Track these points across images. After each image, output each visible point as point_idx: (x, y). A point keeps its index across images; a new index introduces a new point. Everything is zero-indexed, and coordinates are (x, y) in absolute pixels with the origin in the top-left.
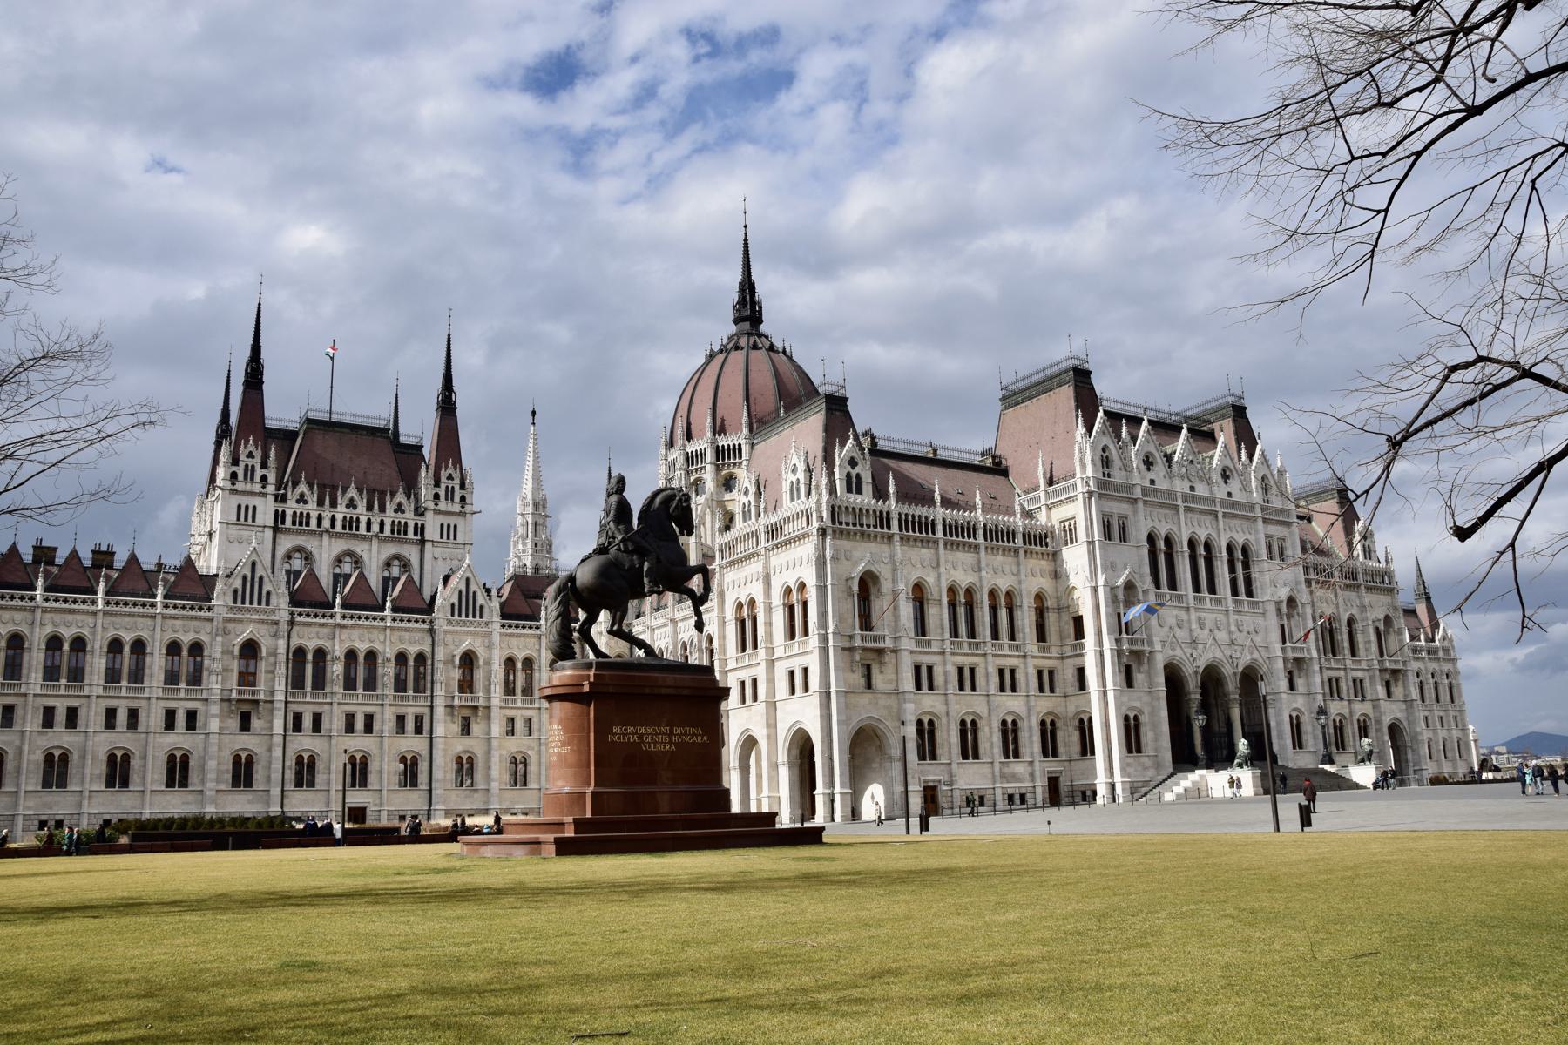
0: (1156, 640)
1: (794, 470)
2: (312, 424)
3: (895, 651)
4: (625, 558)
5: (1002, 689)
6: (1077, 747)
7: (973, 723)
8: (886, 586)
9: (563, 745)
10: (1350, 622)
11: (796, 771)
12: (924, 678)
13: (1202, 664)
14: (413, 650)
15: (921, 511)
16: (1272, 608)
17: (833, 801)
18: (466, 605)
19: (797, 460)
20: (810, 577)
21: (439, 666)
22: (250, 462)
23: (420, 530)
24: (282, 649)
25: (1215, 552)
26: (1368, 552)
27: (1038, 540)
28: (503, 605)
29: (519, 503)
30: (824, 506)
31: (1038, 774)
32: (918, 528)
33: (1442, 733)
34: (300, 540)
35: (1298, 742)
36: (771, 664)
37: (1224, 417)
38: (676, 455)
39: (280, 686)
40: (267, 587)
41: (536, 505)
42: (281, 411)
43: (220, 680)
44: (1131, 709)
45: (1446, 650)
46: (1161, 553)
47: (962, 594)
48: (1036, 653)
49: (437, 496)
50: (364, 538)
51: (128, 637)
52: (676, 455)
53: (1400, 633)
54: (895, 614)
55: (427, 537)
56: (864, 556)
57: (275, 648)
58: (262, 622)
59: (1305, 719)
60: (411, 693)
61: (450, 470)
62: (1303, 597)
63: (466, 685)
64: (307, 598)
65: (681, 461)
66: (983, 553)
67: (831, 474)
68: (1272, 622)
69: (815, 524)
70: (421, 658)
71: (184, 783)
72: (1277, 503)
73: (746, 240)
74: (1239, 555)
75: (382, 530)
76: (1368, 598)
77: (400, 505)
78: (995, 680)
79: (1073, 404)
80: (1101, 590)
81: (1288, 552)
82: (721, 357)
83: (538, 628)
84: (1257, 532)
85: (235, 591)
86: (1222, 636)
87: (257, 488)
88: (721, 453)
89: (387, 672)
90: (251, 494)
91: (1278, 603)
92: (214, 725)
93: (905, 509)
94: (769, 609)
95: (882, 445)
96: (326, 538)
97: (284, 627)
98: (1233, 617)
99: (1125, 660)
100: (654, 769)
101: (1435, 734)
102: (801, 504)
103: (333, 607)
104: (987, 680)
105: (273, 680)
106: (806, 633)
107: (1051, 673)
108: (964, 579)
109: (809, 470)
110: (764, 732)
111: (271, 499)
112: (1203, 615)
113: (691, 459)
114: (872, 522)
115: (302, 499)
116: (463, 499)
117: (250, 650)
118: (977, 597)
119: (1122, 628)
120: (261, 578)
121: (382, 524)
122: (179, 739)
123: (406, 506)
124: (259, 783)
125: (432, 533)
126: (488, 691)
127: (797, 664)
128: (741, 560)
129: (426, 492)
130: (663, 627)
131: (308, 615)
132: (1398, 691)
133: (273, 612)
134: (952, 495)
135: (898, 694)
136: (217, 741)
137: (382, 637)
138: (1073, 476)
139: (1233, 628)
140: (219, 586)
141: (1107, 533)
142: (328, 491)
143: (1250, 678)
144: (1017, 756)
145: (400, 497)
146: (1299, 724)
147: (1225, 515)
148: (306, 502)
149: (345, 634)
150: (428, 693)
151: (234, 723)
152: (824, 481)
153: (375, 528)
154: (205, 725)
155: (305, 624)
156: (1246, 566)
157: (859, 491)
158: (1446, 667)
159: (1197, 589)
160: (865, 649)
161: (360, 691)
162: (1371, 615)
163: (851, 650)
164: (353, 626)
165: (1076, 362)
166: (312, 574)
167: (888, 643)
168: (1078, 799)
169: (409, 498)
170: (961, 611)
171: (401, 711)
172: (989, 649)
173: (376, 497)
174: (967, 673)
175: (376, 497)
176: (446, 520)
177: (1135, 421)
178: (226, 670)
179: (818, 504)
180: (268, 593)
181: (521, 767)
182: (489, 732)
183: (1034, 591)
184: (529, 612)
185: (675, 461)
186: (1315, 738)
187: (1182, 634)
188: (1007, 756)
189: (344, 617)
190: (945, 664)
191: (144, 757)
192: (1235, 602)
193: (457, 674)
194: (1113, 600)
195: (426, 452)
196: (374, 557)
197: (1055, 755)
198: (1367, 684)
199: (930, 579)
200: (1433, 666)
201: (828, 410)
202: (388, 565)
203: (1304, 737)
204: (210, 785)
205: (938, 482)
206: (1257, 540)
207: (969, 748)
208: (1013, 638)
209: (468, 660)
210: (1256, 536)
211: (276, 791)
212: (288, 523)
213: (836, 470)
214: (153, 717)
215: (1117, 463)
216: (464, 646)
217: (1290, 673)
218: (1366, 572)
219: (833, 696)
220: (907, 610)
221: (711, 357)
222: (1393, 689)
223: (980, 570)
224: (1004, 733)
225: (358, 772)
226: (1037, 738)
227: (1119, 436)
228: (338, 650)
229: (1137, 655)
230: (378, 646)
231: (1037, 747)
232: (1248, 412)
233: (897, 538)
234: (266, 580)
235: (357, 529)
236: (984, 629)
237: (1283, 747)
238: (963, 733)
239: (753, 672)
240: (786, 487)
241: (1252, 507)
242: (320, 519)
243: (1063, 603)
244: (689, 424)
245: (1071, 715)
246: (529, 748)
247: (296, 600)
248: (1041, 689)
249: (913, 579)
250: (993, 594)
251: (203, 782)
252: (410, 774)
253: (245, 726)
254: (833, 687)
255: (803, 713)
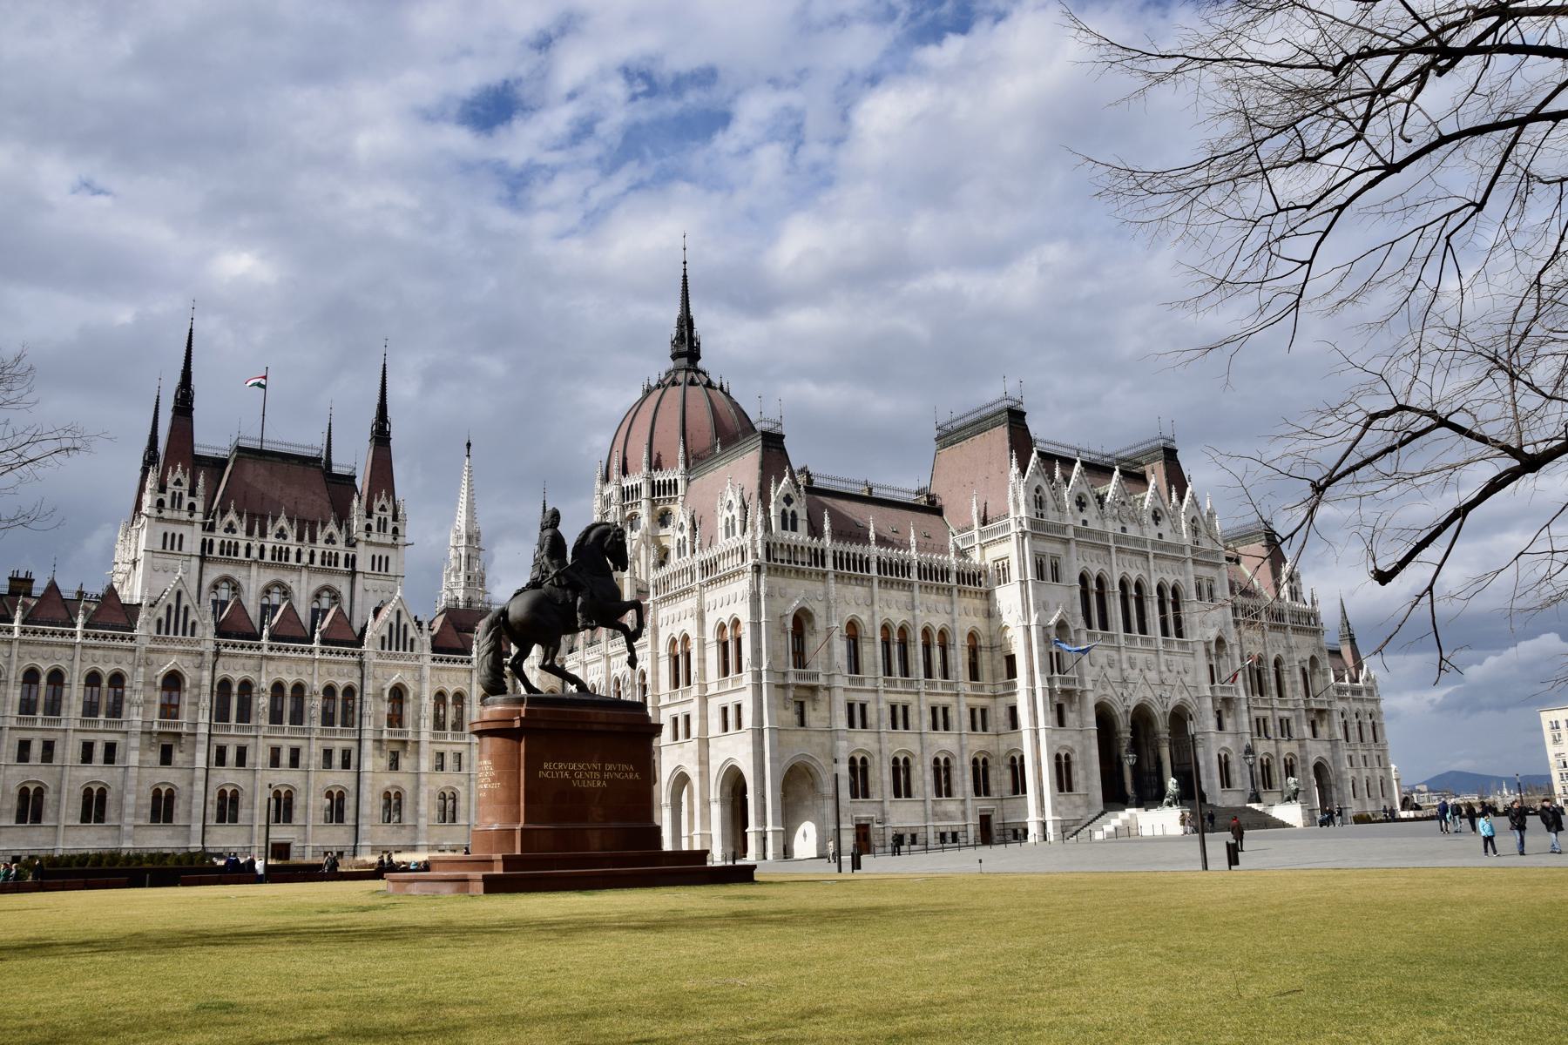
0: (1088, 679)
1: (730, 507)
2: (243, 452)
3: (828, 689)
4: (559, 593)
5: (935, 727)
6: (1008, 786)
7: (906, 761)
8: (820, 623)
9: (493, 780)
10: (1277, 663)
11: (729, 808)
12: (857, 715)
13: (1132, 704)
14: (341, 683)
15: (855, 549)
16: (1201, 649)
17: (765, 839)
18: (397, 638)
19: (733, 497)
20: (744, 613)
21: (368, 699)
22: (177, 489)
23: (351, 561)
24: (207, 681)
25: (1146, 592)
26: (1295, 594)
27: (971, 578)
28: (434, 639)
29: (452, 535)
30: (759, 543)
31: (969, 812)
32: (853, 567)
33: (1366, 772)
34: (228, 570)
35: (1226, 781)
36: (704, 700)
37: (1155, 459)
38: (612, 489)
39: (204, 718)
40: (192, 617)
41: (469, 538)
42: (211, 438)
43: (141, 712)
44: (1064, 747)
45: (1370, 691)
46: (1092, 593)
47: (896, 632)
48: (969, 692)
49: (368, 527)
50: (293, 568)
51: (45, 667)
52: (612, 489)
53: (1325, 673)
54: (828, 652)
55: (358, 568)
56: (798, 593)
57: (200, 680)
58: (187, 653)
59: (1233, 758)
60: (338, 726)
61: (383, 501)
62: (1232, 638)
63: (396, 719)
64: (234, 628)
65: (616, 495)
66: (917, 591)
67: (766, 511)
68: (1202, 663)
69: (750, 561)
70: (349, 691)
71: (100, 818)
72: (1206, 545)
73: (685, 276)
74: (1169, 595)
75: (312, 561)
76: (1294, 639)
77: (331, 535)
78: (928, 718)
79: (1007, 444)
80: (1033, 630)
81: (1217, 594)
82: (658, 392)
83: (469, 662)
84: (1187, 573)
85: (160, 621)
86: (1152, 676)
87: (185, 516)
88: (656, 488)
89: (314, 705)
90: (178, 522)
91: (1207, 643)
92: (134, 758)
93: (840, 547)
94: (703, 645)
95: (818, 483)
96: (254, 568)
97: (209, 658)
98: (1163, 657)
99: (1056, 699)
100: (584, 803)
101: (1359, 773)
102: (737, 540)
103: (259, 637)
104: (921, 718)
105: (197, 713)
106: (739, 670)
107: (983, 711)
108: (897, 617)
109: (744, 507)
110: (697, 769)
111: (198, 527)
112: (1133, 655)
113: (626, 494)
114: (807, 560)
115: (230, 528)
116: (395, 530)
117: (173, 681)
118: (911, 636)
119: (1055, 663)
120: (186, 608)
121: (312, 555)
122: (96, 772)
123: (337, 536)
124: (179, 820)
125: (363, 564)
126: (417, 724)
127: (730, 701)
128: (675, 596)
129: (357, 522)
130: (596, 662)
131: (234, 646)
132: (1323, 731)
133: (198, 643)
134: (887, 533)
135: (831, 731)
136: (136, 774)
137: (310, 670)
138: (1007, 516)
139: (1163, 668)
140: (142, 616)
141: (1040, 574)
142: (257, 520)
143: (1179, 717)
144: (949, 794)
145: (332, 528)
146: (1227, 763)
147: (1156, 556)
148: (234, 532)
149: (272, 666)
150: (356, 727)
151: (155, 756)
152: (760, 517)
153: (305, 558)
154: (125, 759)
155: (231, 656)
156: (1176, 607)
157: (794, 529)
158: (1370, 707)
159: (1128, 629)
160: (798, 687)
161: (287, 724)
162: (1297, 656)
163: (784, 687)
164: (281, 658)
165: (1010, 403)
166: (239, 605)
167: (822, 681)
168: (1010, 837)
170: (895, 649)
171: (329, 745)
172: (922, 687)
173: (307, 527)
174: (900, 711)
175: (307, 527)
176: (378, 552)
177: (1068, 463)
178: (147, 701)
179: (754, 541)
180: (194, 624)
181: (450, 803)
182: (418, 767)
183: (967, 630)
184: (459, 644)
185: (610, 496)
186: (1243, 777)
187: (1112, 673)
188: (939, 794)
189: (271, 649)
190: (878, 702)
191: (59, 792)
192: (1165, 642)
193: (386, 708)
194: (1046, 639)
195: (358, 482)
196: (303, 587)
197: (987, 793)
198: (1293, 724)
199: (864, 618)
200: (1357, 706)
201: (764, 446)
202: (318, 596)
203: (1232, 777)
204: (128, 820)
205: (873, 520)
206: (1187, 581)
207: (902, 786)
208: (946, 676)
209: (398, 694)
210: (1186, 577)
211: (197, 827)
212: (216, 553)
213: (772, 507)
214: (69, 750)
215: (1050, 503)
216: (394, 680)
217: (1219, 712)
218: (1292, 614)
219: (766, 732)
220: (840, 648)
221: (648, 392)
222: (1318, 728)
223: (913, 608)
224: (937, 771)
225: (283, 806)
226: (969, 776)
227: (1052, 477)
228: (265, 682)
229: (1068, 694)
230: (305, 679)
231: (969, 786)
232: (1179, 456)
233: (831, 576)
234: (191, 610)
235: (287, 559)
236: (918, 668)
237: (1211, 786)
238: (896, 771)
239: (685, 709)
240: (721, 523)
241: (1182, 548)
242: (248, 548)
243: (996, 642)
244: (625, 459)
245: (1003, 753)
246: (459, 783)
247: (222, 631)
248: (974, 728)
249: (847, 617)
250: (926, 632)
251: (120, 816)
252: (336, 809)
253: (166, 759)
254: (766, 725)
255: (736, 750)
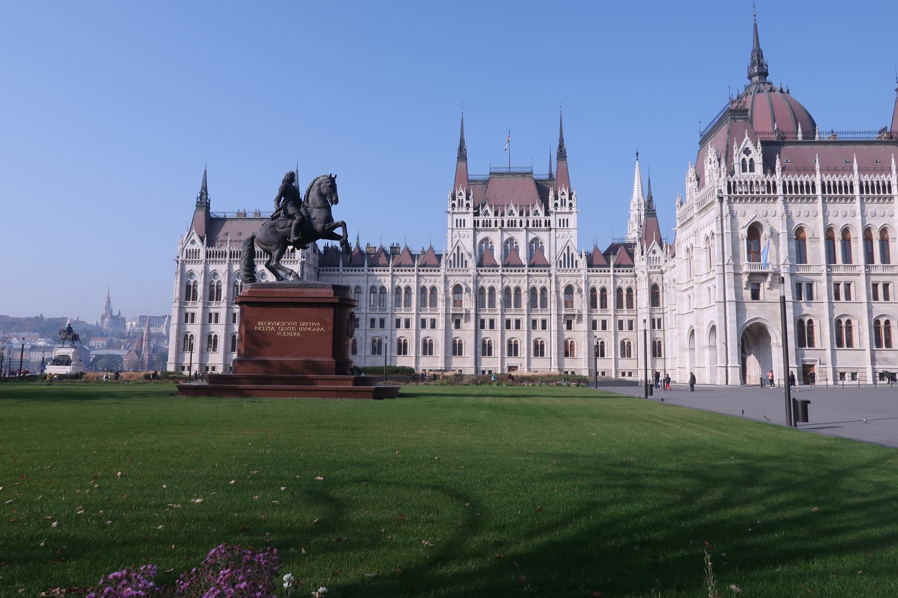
17: (727, 371)
23: (548, 223)
49: (556, 205)
55: (552, 226)
87: (464, 210)
89: (525, 298)
116: (571, 205)
123: (540, 212)
157: (752, 169)
169: (541, 206)
225: (513, 349)
